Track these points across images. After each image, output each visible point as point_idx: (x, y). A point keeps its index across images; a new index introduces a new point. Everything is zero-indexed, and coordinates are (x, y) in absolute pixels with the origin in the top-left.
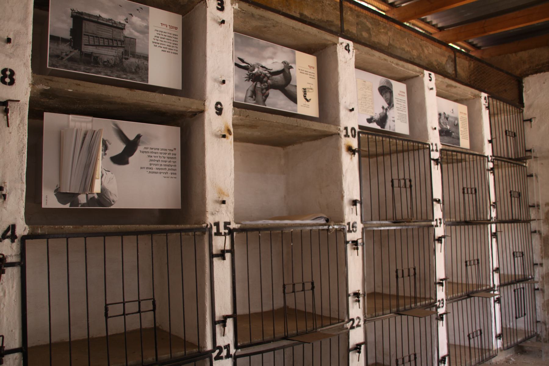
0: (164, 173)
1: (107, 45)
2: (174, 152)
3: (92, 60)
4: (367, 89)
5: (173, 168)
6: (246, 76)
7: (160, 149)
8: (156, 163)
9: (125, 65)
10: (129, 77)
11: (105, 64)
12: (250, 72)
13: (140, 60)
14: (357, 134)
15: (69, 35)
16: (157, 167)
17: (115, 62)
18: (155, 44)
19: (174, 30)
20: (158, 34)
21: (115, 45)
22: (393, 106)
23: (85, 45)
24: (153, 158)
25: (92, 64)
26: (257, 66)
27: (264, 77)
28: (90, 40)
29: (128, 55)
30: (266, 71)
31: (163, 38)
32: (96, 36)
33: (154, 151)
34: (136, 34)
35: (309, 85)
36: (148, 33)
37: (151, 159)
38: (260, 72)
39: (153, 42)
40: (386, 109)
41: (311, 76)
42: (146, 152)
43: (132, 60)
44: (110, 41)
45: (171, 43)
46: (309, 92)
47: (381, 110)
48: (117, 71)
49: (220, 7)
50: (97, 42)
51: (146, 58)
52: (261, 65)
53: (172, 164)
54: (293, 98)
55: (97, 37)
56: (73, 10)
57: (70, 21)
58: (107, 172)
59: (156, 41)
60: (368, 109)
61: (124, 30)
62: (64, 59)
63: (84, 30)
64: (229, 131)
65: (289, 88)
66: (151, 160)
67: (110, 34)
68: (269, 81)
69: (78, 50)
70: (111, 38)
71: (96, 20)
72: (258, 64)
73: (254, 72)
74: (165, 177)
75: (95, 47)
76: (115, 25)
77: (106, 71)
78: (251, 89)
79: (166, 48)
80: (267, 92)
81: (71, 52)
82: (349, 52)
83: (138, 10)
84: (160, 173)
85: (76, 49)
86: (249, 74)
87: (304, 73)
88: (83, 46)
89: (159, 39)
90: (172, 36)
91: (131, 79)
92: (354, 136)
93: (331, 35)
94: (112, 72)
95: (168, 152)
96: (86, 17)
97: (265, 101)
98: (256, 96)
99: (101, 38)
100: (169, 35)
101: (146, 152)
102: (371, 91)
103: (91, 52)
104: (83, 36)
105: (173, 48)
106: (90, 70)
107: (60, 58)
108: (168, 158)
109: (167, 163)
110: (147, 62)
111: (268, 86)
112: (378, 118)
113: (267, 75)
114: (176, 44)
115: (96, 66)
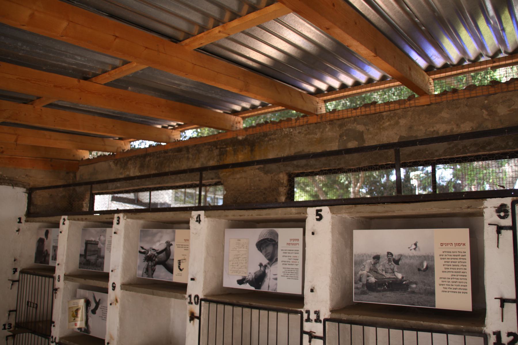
4: (241, 248)
12: (146, 255)
14: (199, 301)
22: (277, 260)
27: (153, 257)
34: (102, 245)
35: (184, 256)
40: (266, 266)
41: (185, 248)
43: (100, 260)
46: (183, 262)
47: (258, 268)
54: (170, 270)
60: (240, 270)
65: (169, 262)
66: (103, 313)
68: (156, 259)
72: (151, 248)
73: (148, 255)
78: (146, 267)
82: (199, 223)
92: (196, 303)
93: (186, 212)
96: (89, 242)
97: (153, 274)
102: (246, 248)
112: (252, 279)
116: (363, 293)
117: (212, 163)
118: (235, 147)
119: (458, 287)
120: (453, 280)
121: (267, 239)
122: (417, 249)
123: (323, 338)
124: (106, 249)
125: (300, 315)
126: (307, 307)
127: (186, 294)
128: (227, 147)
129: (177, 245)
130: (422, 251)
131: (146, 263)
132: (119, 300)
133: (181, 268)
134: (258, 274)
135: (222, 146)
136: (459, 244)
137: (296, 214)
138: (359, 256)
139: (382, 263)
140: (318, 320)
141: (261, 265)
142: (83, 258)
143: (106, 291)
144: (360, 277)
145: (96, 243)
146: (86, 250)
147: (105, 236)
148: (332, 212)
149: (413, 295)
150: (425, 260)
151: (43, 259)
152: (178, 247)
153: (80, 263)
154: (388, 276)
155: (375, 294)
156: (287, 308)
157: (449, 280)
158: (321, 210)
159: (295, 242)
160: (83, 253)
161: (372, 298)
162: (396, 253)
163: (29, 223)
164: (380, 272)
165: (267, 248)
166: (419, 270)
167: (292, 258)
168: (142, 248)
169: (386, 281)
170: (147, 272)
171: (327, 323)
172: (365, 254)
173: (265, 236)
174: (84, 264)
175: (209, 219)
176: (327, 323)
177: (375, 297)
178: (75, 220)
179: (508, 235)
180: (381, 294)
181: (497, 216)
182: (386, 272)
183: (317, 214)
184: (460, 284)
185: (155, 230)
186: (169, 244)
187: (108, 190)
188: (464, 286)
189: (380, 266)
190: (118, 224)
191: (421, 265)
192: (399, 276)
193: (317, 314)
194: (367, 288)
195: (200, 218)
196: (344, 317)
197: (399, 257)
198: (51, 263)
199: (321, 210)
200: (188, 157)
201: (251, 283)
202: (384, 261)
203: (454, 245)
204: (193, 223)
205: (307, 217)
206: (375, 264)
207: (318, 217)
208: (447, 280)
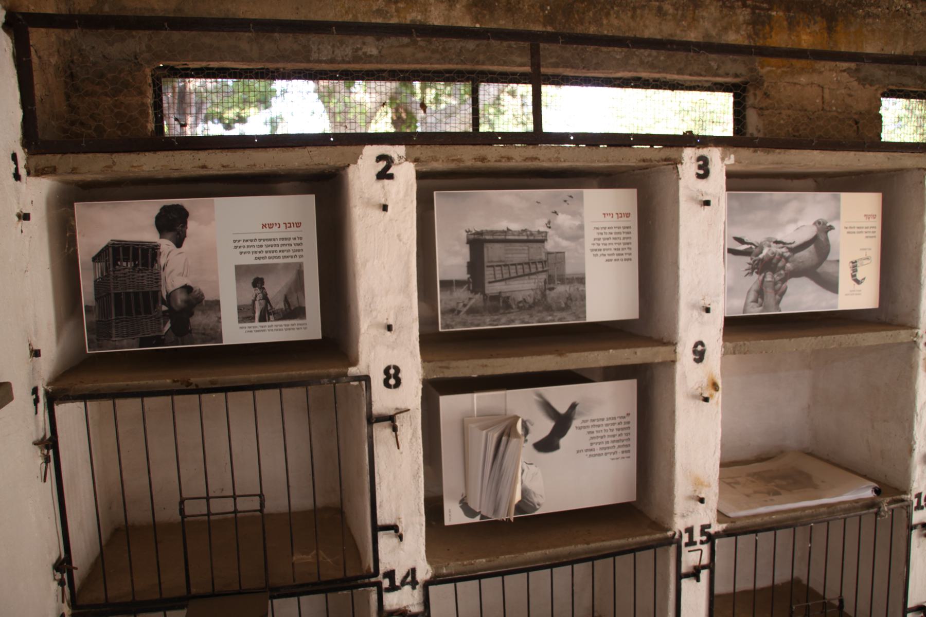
0: (611, 453)
1: (522, 274)
2: (627, 419)
3: (501, 304)
5: (625, 443)
7: (606, 419)
8: (599, 440)
9: (549, 300)
10: (556, 319)
11: (521, 305)
12: (755, 258)
13: (572, 285)
15: (466, 272)
16: (601, 446)
17: (534, 300)
18: (595, 253)
19: (625, 219)
20: (598, 234)
21: (533, 270)
23: (490, 282)
24: (595, 435)
25: (502, 311)
26: (768, 243)
27: (779, 260)
28: (497, 272)
29: (554, 283)
30: (782, 247)
31: (608, 239)
32: (503, 263)
33: (596, 423)
34: (565, 243)
36: (583, 237)
37: (592, 435)
38: (773, 253)
39: (592, 250)
41: (868, 235)
42: (585, 427)
43: (561, 289)
44: (526, 266)
45: (619, 244)
46: (862, 265)
48: (539, 312)
49: (701, 172)
50: (506, 273)
51: (581, 280)
52: (774, 240)
53: (624, 437)
54: (831, 285)
55: (505, 265)
56: (469, 231)
57: (466, 250)
58: (529, 466)
59: (596, 247)
61: (546, 243)
62: (461, 313)
63: (486, 260)
64: (715, 386)
65: (826, 268)
66: (592, 438)
67: (525, 255)
68: (788, 265)
69: (479, 294)
70: (527, 260)
71: (503, 237)
72: (769, 240)
73: (761, 256)
74: (613, 459)
75: (503, 283)
76: (531, 238)
77: (521, 317)
78: (756, 287)
79: (613, 254)
80: (784, 285)
81: (470, 299)
83: (565, 201)
84: (606, 454)
85: (476, 293)
86: (752, 262)
87: (854, 233)
88: (487, 285)
89: (602, 241)
90: (621, 230)
91: (560, 320)
94: (531, 316)
95: (618, 420)
96: (487, 237)
97: (778, 302)
98: (763, 299)
99: (512, 265)
100: (617, 230)
101: (585, 427)
103: (499, 291)
104: (486, 269)
105: (623, 252)
106: (499, 320)
107: (456, 312)
108: (618, 430)
109: (617, 438)
110: (582, 286)
111: (786, 274)
113: (785, 254)
114: (628, 244)
115: (507, 312)
117: (732, 38)
118: (792, 14)
124: (588, 256)
128: (771, 9)
129: (846, 228)
131: (755, 277)
133: (859, 277)
135: (758, 4)
145: (539, 240)
147: (577, 214)
152: (849, 233)
168: (741, 241)
170: (760, 300)
186: (824, 228)
187: (309, 61)
200: (660, 9)
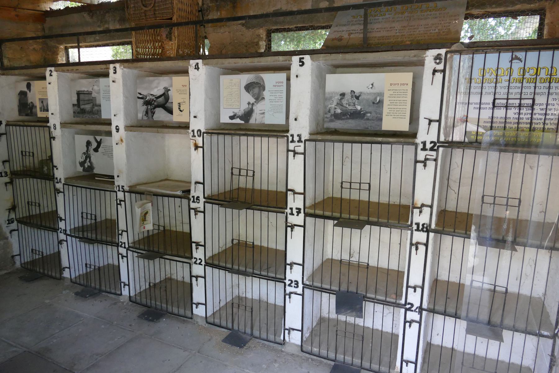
6: (143, 103)
14: (202, 134)
27: (152, 101)
34: (96, 95)
35: (183, 99)
43: (96, 108)
51: (100, 106)
54: (170, 112)
57: (76, 96)
64: (122, 140)
65: (168, 105)
68: (155, 103)
72: (149, 94)
73: (146, 99)
78: (145, 110)
82: (198, 70)
92: (199, 136)
96: (80, 92)
97: (153, 116)
116: (331, 121)
119: (400, 114)
120: (397, 110)
121: (254, 82)
122: (373, 88)
123: (304, 154)
124: (102, 98)
125: (286, 138)
126: (291, 132)
127: (189, 129)
130: (376, 90)
131: (145, 107)
132: (124, 140)
133: (181, 109)
134: (247, 110)
136: (404, 84)
137: (283, 61)
138: (329, 93)
139: (346, 99)
140: (300, 141)
141: (249, 103)
142: (76, 108)
143: (109, 134)
144: (330, 109)
145: (90, 93)
146: (78, 100)
147: (98, 86)
148: (312, 59)
149: (368, 121)
150: (378, 96)
151: (29, 111)
153: (74, 112)
154: (350, 108)
155: (340, 121)
156: (276, 134)
157: (394, 110)
158: (303, 58)
159: (280, 84)
160: (76, 103)
161: (338, 125)
162: (357, 91)
163: (5, 76)
164: (345, 105)
165: (254, 90)
166: (373, 103)
167: (278, 96)
168: (140, 94)
169: (348, 112)
171: (307, 142)
172: (334, 92)
173: (251, 80)
174: (78, 113)
175: (206, 66)
176: (307, 142)
177: (340, 124)
178: (63, 71)
179: (439, 76)
180: (345, 121)
181: (434, 63)
182: (349, 105)
183: (300, 62)
184: (402, 112)
185: (151, 78)
186: (167, 90)
188: (404, 113)
189: (344, 101)
190: (115, 73)
191: (375, 99)
192: (359, 108)
193: (299, 137)
194: (334, 117)
195: (198, 66)
196: (319, 137)
197: (359, 94)
198: (40, 114)
199: (303, 58)
201: (241, 118)
202: (348, 97)
203: (400, 85)
204: (192, 71)
205: (291, 64)
206: (341, 99)
207: (301, 64)
208: (393, 110)
